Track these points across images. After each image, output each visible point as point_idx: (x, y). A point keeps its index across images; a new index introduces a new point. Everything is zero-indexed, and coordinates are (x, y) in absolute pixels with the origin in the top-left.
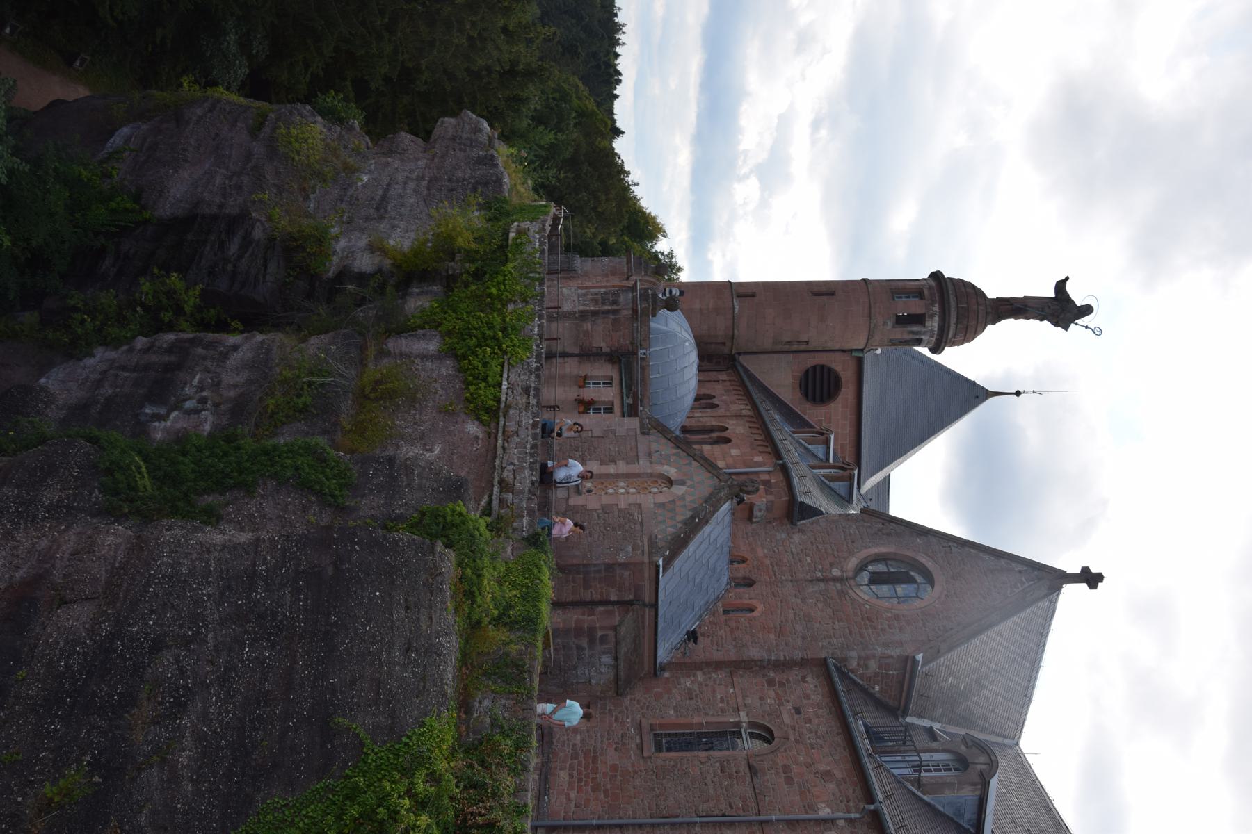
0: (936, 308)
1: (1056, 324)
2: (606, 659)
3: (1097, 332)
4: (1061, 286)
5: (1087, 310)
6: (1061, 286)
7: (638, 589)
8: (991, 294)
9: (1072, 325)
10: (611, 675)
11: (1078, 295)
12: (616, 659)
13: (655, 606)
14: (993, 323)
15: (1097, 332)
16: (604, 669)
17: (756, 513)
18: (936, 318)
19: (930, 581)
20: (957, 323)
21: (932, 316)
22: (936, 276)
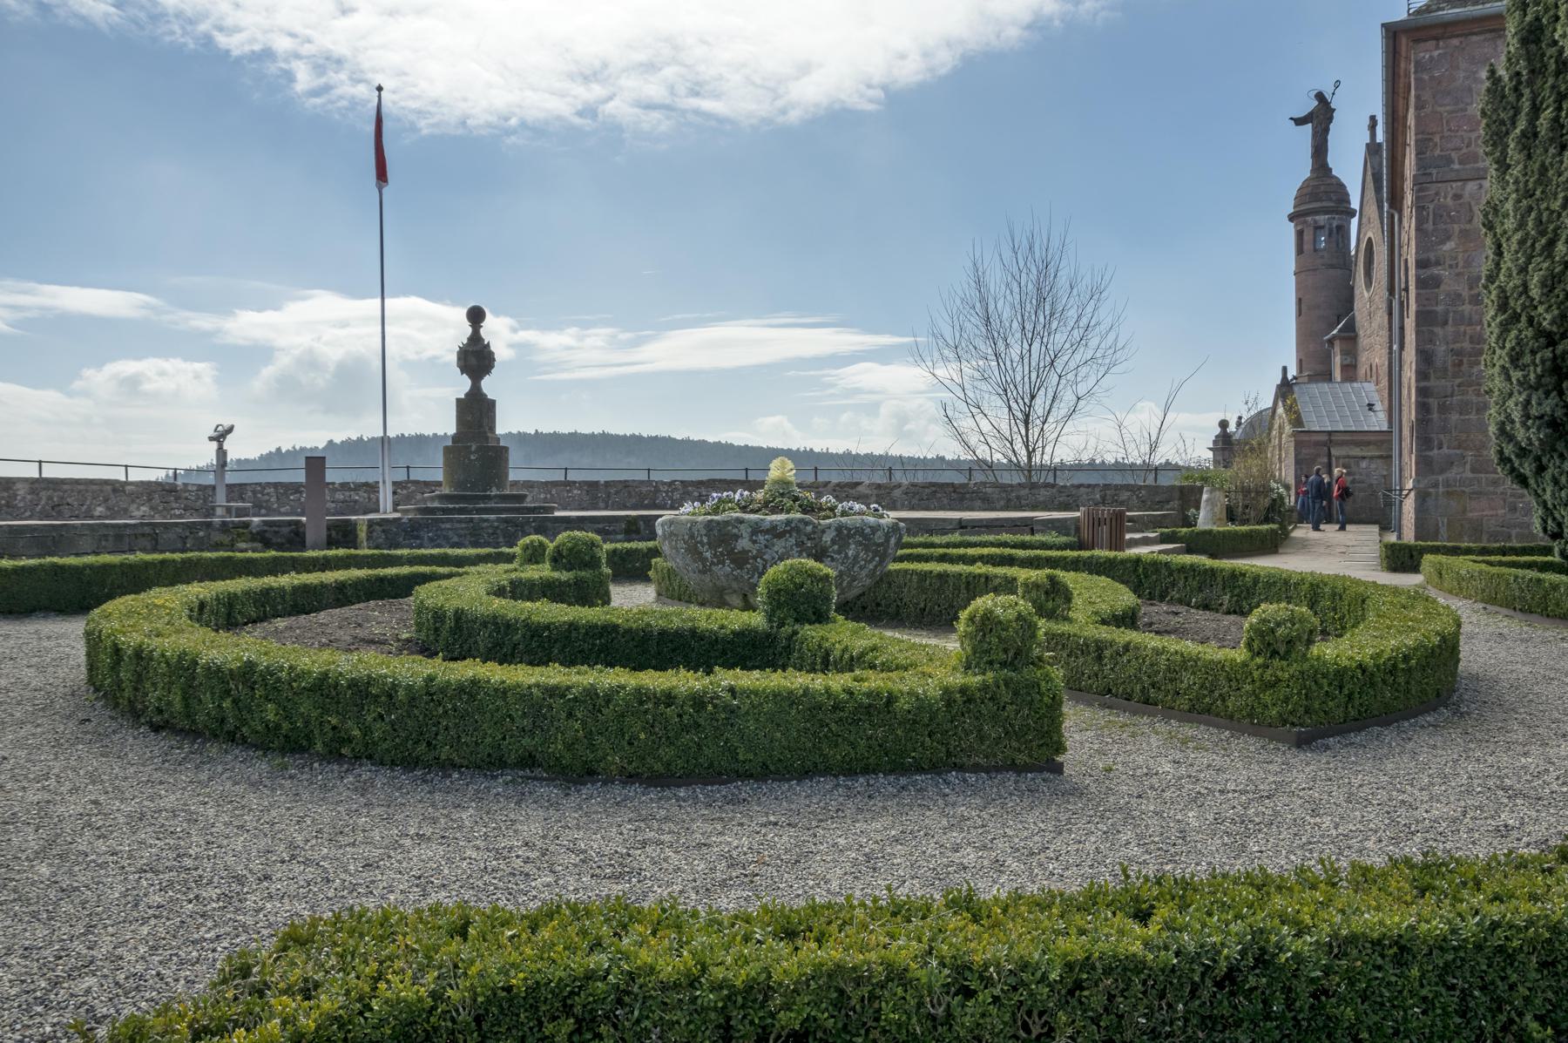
0: (1309, 219)
1: (1330, 119)
2: (1364, 464)
3: (1337, 84)
4: (1299, 122)
5: (1320, 96)
6: (1299, 122)
7: (1317, 444)
8: (1308, 175)
9: (1333, 106)
10: (1379, 461)
11: (1309, 105)
12: (1364, 458)
13: (1330, 433)
14: (1331, 170)
15: (1337, 84)
16: (1373, 466)
17: (1348, 362)
18: (1317, 218)
19: (1370, 239)
20: (1321, 201)
21: (1315, 222)
22: (1291, 218)
